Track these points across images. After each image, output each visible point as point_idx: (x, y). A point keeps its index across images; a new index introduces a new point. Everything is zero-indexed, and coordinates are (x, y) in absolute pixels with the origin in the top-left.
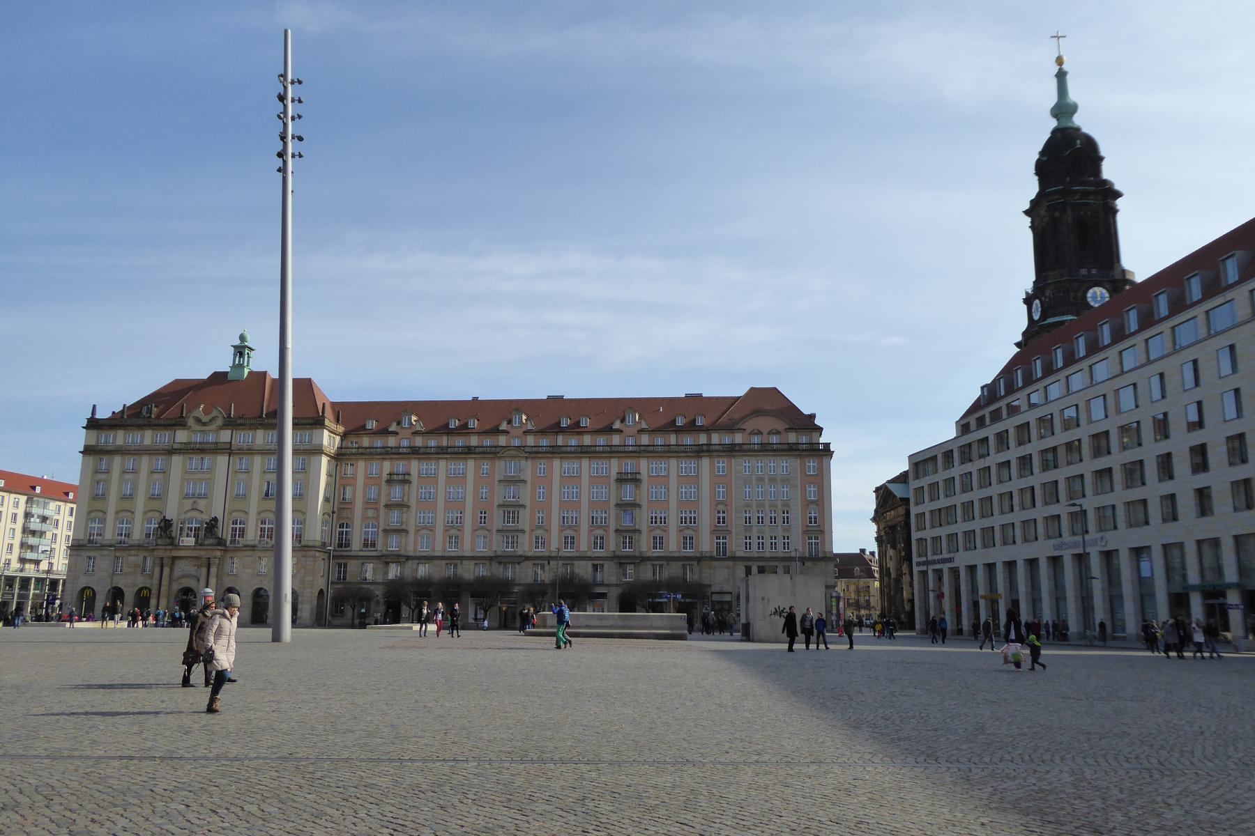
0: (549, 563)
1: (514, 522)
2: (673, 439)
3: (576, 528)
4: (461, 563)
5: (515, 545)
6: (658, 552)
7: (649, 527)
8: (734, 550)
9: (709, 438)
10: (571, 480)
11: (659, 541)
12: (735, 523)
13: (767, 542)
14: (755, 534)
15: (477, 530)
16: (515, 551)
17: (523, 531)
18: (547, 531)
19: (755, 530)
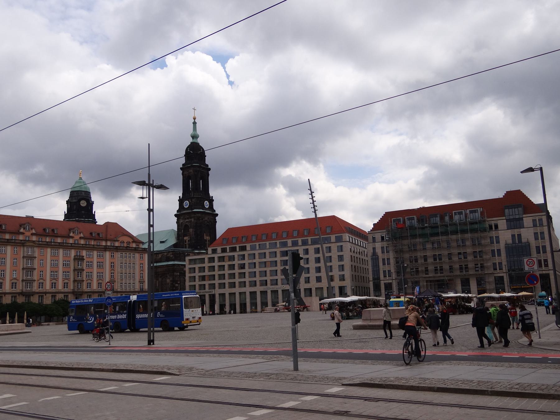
0: (46, 295)
1: (30, 276)
2: (92, 243)
3: (57, 279)
4: (5, 296)
5: (31, 287)
6: (89, 290)
7: (86, 279)
8: (117, 288)
9: (106, 243)
10: (55, 257)
11: (89, 285)
12: (117, 277)
13: (128, 285)
14: (124, 282)
15: (12, 280)
16: (31, 290)
17: (35, 280)
18: (44, 280)
19: (124, 280)
